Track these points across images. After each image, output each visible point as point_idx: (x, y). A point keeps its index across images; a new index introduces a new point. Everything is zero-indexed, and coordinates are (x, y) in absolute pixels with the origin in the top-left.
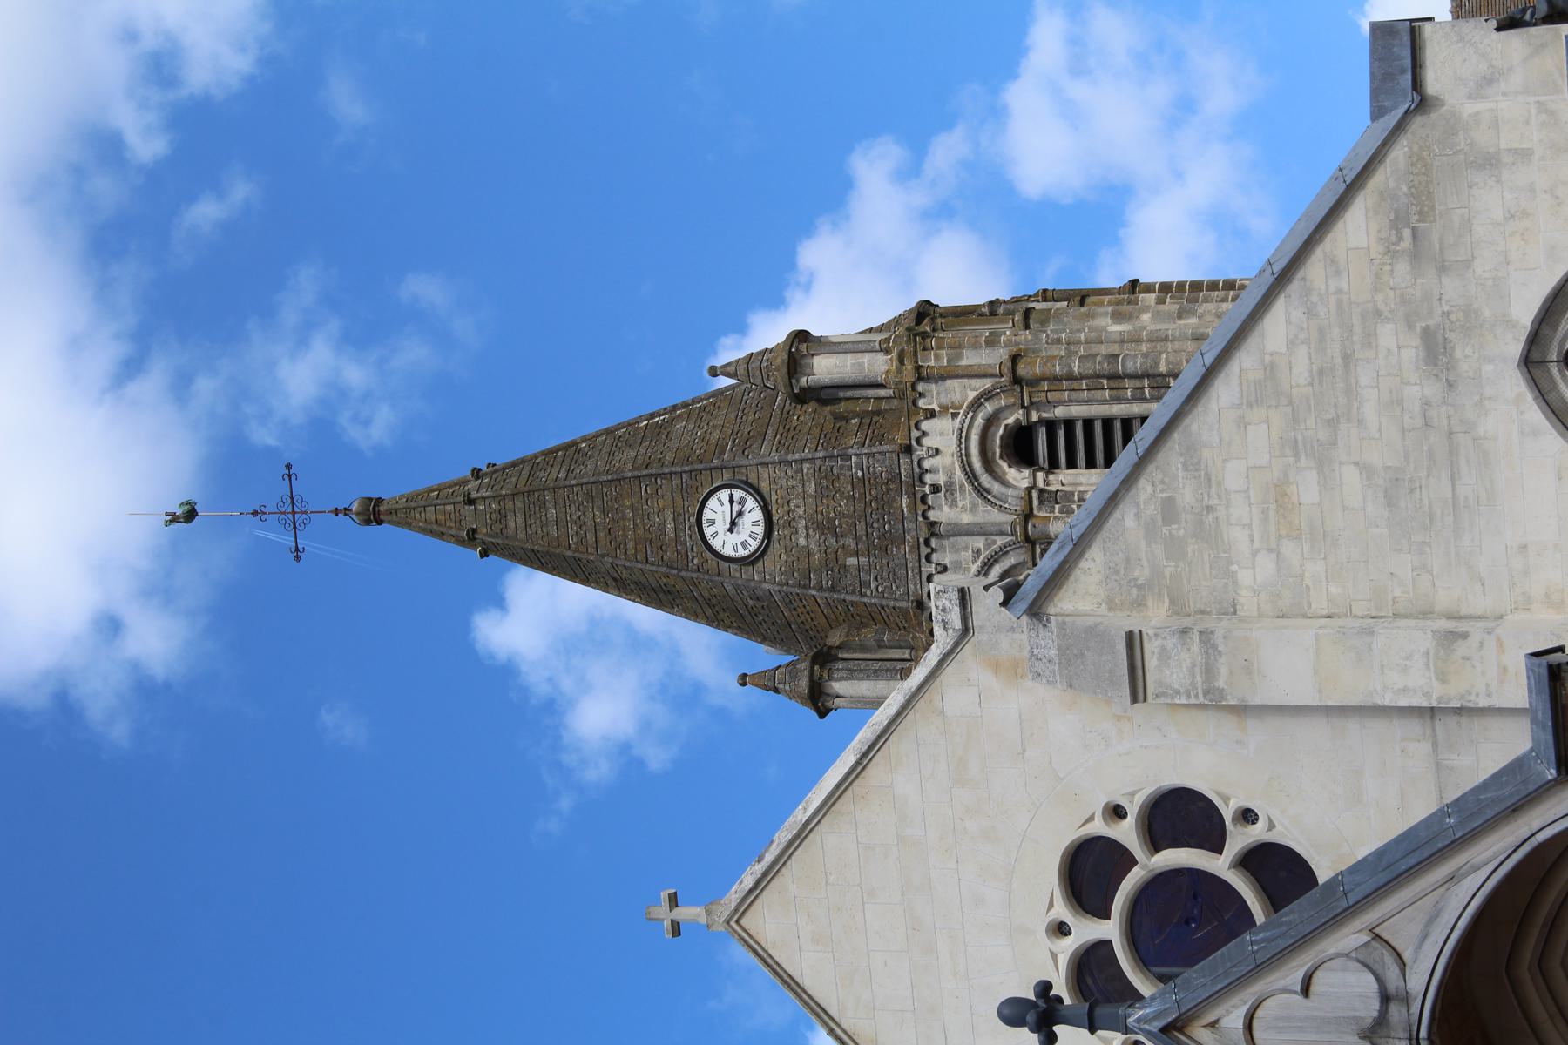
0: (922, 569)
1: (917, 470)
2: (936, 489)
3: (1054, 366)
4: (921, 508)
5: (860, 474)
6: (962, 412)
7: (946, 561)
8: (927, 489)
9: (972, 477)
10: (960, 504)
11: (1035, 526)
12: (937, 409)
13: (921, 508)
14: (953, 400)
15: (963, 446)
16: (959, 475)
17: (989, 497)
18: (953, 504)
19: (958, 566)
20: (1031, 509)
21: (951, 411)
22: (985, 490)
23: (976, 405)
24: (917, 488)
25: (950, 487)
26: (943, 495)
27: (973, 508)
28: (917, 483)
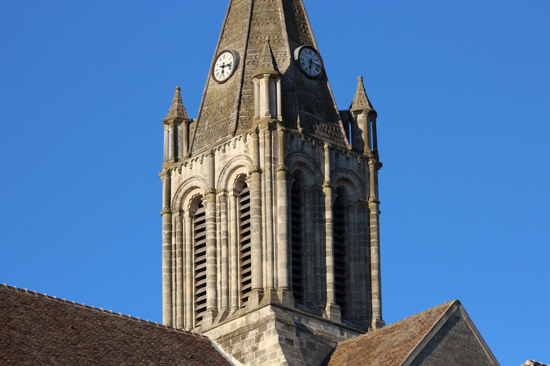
0: (200, 154)
1: (228, 142)
2: (224, 151)
3: (254, 189)
4: (217, 147)
5: (230, 117)
6: (246, 154)
7: (204, 163)
8: (223, 148)
9: (227, 166)
10: (220, 163)
11: (209, 197)
12: (247, 143)
13: (217, 147)
14: (250, 150)
15: (237, 158)
16: (228, 159)
17: (222, 175)
18: (220, 160)
19: (202, 169)
20: (218, 193)
21: (247, 149)
22: (224, 172)
23: (248, 158)
24: (223, 144)
25: (225, 157)
26: (222, 155)
27: (219, 169)
28: (224, 143)
